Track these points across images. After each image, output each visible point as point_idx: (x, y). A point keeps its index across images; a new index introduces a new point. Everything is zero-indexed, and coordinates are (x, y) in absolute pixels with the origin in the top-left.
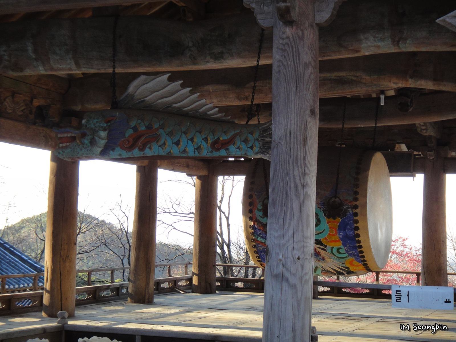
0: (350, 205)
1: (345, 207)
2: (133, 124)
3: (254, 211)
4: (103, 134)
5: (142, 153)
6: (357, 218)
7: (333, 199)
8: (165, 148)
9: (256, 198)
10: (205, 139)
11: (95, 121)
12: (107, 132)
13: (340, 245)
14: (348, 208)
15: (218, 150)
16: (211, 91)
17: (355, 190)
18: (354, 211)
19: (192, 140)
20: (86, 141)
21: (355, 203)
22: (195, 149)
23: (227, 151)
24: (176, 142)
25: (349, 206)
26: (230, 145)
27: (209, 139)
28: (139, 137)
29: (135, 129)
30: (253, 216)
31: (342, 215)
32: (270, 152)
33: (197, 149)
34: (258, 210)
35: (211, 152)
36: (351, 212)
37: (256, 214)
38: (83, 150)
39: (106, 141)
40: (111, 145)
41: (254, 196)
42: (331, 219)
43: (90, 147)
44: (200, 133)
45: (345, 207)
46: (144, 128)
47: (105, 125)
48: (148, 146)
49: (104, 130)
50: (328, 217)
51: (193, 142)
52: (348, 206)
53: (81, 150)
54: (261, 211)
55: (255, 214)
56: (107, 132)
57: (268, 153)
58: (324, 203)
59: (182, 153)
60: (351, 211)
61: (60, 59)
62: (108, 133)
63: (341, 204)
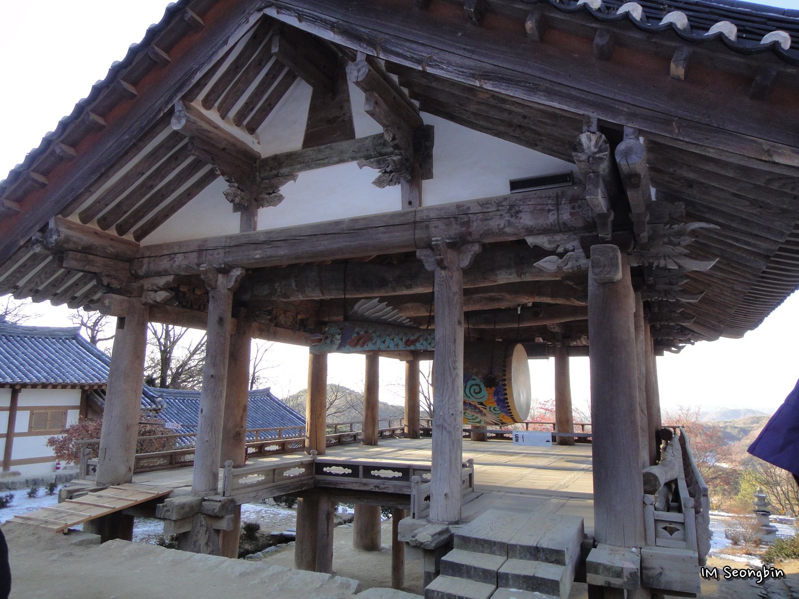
2: (357, 330)
4: (339, 337)
6: (505, 387)
12: (340, 336)
13: (495, 405)
19: (393, 340)
20: (328, 341)
29: (358, 333)
35: (405, 347)
42: (489, 388)
44: (398, 335)
46: (363, 333)
49: (339, 334)
50: (487, 387)
56: (340, 336)
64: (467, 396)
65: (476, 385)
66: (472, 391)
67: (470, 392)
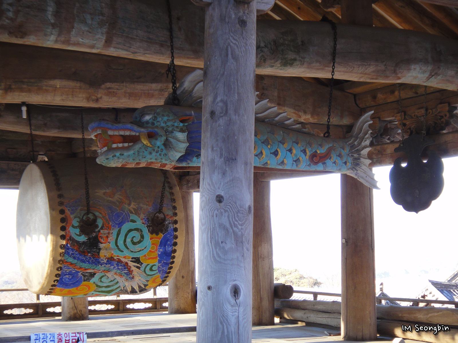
0: (170, 220)
1: (167, 223)
3: (67, 228)
6: (177, 233)
8: (262, 158)
9: (69, 213)
10: (303, 152)
11: (165, 118)
12: (186, 134)
13: (156, 262)
14: (170, 223)
16: (58, 87)
17: (174, 204)
18: (174, 227)
19: (290, 150)
20: (159, 143)
21: (175, 218)
22: (293, 161)
23: (324, 166)
24: (274, 152)
25: (170, 221)
26: (327, 159)
27: (307, 152)
30: (66, 234)
31: (164, 230)
32: (357, 168)
33: (295, 161)
34: (73, 227)
35: (309, 165)
36: (172, 227)
37: (71, 231)
38: (154, 154)
39: (188, 144)
40: (195, 150)
41: (67, 212)
43: (165, 151)
44: (297, 143)
45: (167, 223)
47: (181, 124)
49: (182, 131)
50: (152, 233)
51: (292, 153)
52: (169, 221)
53: (151, 153)
54: (78, 228)
55: (69, 232)
57: (356, 170)
58: (148, 219)
59: (279, 164)
60: (171, 227)
61: (88, 31)
63: (164, 220)
64: (119, 249)
65: (137, 230)
66: (128, 240)
67: (125, 241)
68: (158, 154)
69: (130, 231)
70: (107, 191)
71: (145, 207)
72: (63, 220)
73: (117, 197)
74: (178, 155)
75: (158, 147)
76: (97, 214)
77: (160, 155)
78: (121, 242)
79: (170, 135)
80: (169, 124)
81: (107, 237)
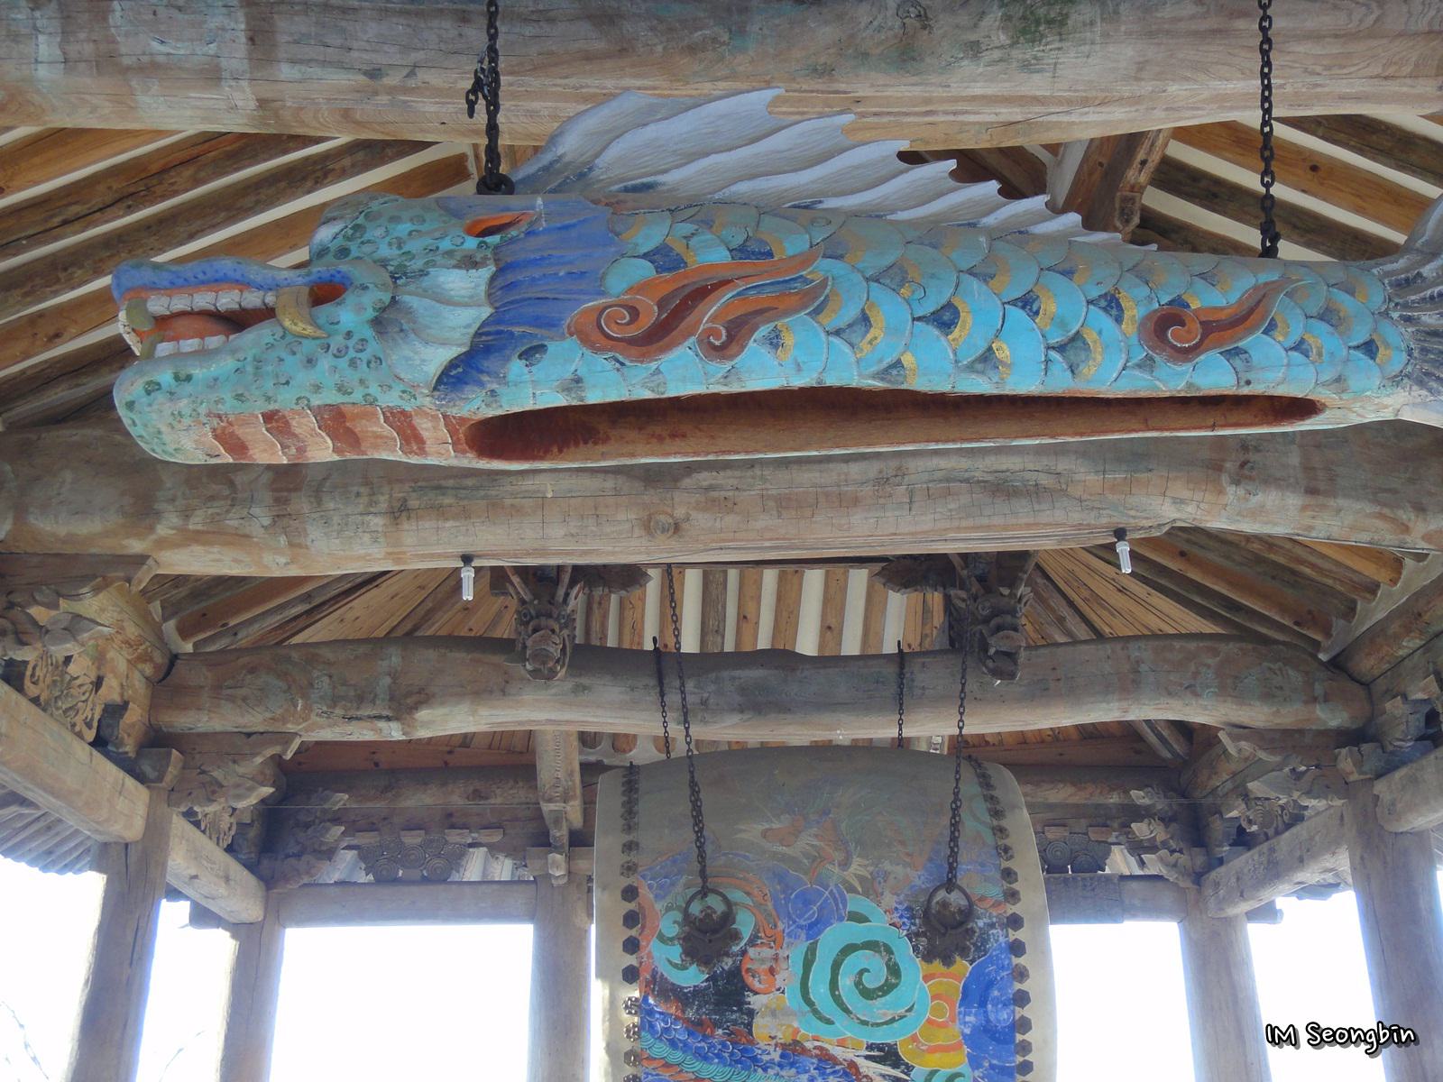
0: (994, 914)
1: (980, 923)
3: (643, 943)
5: (719, 368)
6: (1021, 961)
7: (941, 894)
8: (870, 343)
9: (651, 896)
10: (1103, 303)
11: (403, 229)
12: (486, 273)
14: (992, 926)
15: (1186, 354)
16: (549, 495)
17: (1005, 864)
18: (1011, 938)
19: (1027, 302)
20: (350, 315)
21: (1011, 909)
22: (1049, 348)
23: (1238, 362)
24: (933, 313)
25: (994, 920)
26: (1250, 331)
28: (702, 293)
30: (641, 963)
31: (973, 949)
33: (1061, 348)
34: (663, 939)
35: (1147, 364)
36: (1002, 939)
37: (656, 954)
38: (325, 362)
39: (486, 311)
40: (517, 330)
41: (644, 891)
42: (937, 966)
43: (374, 347)
45: (980, 923)
46: (719, 255)
47: (471, 243)
48: (764, 331)
49: (470, 263)
50: (928, 957)
51: (1037, 313)
52: (990, 917)
53: (310, 362)
54: (676, 942)
55: (650, 955)
58: (909, 909)
59: (970, 368)
60: (1000, 937)
62: (493, 279)
63: (968, 914)
65: (871, 945)
66: (846, 982)
67: (834, 985)
68: (343, 363)
69: (849, 949)
70: (776, 825)
71: (899, 870)
72: (631, 919)
73: (807, 841)
74: (436, 358)
75: (349, 335)
76: (736, 896)
77: (353, 363)
78: (819, 990)
79: (412, 287)
80: (414, 246)
81: (772, 971)
